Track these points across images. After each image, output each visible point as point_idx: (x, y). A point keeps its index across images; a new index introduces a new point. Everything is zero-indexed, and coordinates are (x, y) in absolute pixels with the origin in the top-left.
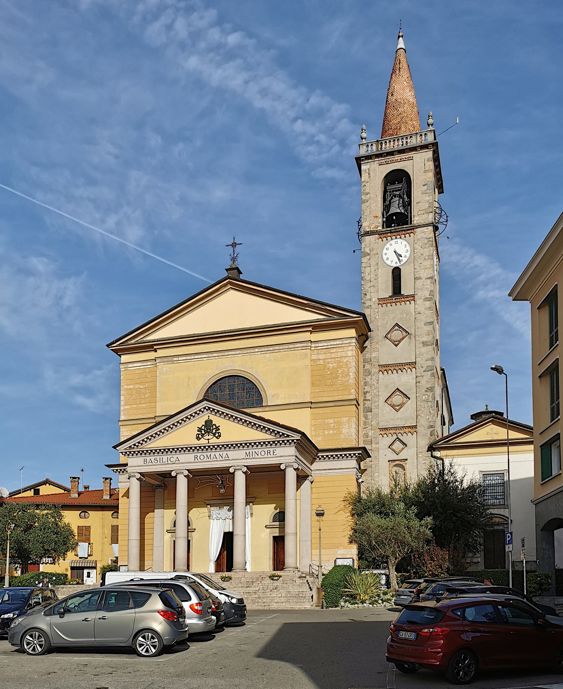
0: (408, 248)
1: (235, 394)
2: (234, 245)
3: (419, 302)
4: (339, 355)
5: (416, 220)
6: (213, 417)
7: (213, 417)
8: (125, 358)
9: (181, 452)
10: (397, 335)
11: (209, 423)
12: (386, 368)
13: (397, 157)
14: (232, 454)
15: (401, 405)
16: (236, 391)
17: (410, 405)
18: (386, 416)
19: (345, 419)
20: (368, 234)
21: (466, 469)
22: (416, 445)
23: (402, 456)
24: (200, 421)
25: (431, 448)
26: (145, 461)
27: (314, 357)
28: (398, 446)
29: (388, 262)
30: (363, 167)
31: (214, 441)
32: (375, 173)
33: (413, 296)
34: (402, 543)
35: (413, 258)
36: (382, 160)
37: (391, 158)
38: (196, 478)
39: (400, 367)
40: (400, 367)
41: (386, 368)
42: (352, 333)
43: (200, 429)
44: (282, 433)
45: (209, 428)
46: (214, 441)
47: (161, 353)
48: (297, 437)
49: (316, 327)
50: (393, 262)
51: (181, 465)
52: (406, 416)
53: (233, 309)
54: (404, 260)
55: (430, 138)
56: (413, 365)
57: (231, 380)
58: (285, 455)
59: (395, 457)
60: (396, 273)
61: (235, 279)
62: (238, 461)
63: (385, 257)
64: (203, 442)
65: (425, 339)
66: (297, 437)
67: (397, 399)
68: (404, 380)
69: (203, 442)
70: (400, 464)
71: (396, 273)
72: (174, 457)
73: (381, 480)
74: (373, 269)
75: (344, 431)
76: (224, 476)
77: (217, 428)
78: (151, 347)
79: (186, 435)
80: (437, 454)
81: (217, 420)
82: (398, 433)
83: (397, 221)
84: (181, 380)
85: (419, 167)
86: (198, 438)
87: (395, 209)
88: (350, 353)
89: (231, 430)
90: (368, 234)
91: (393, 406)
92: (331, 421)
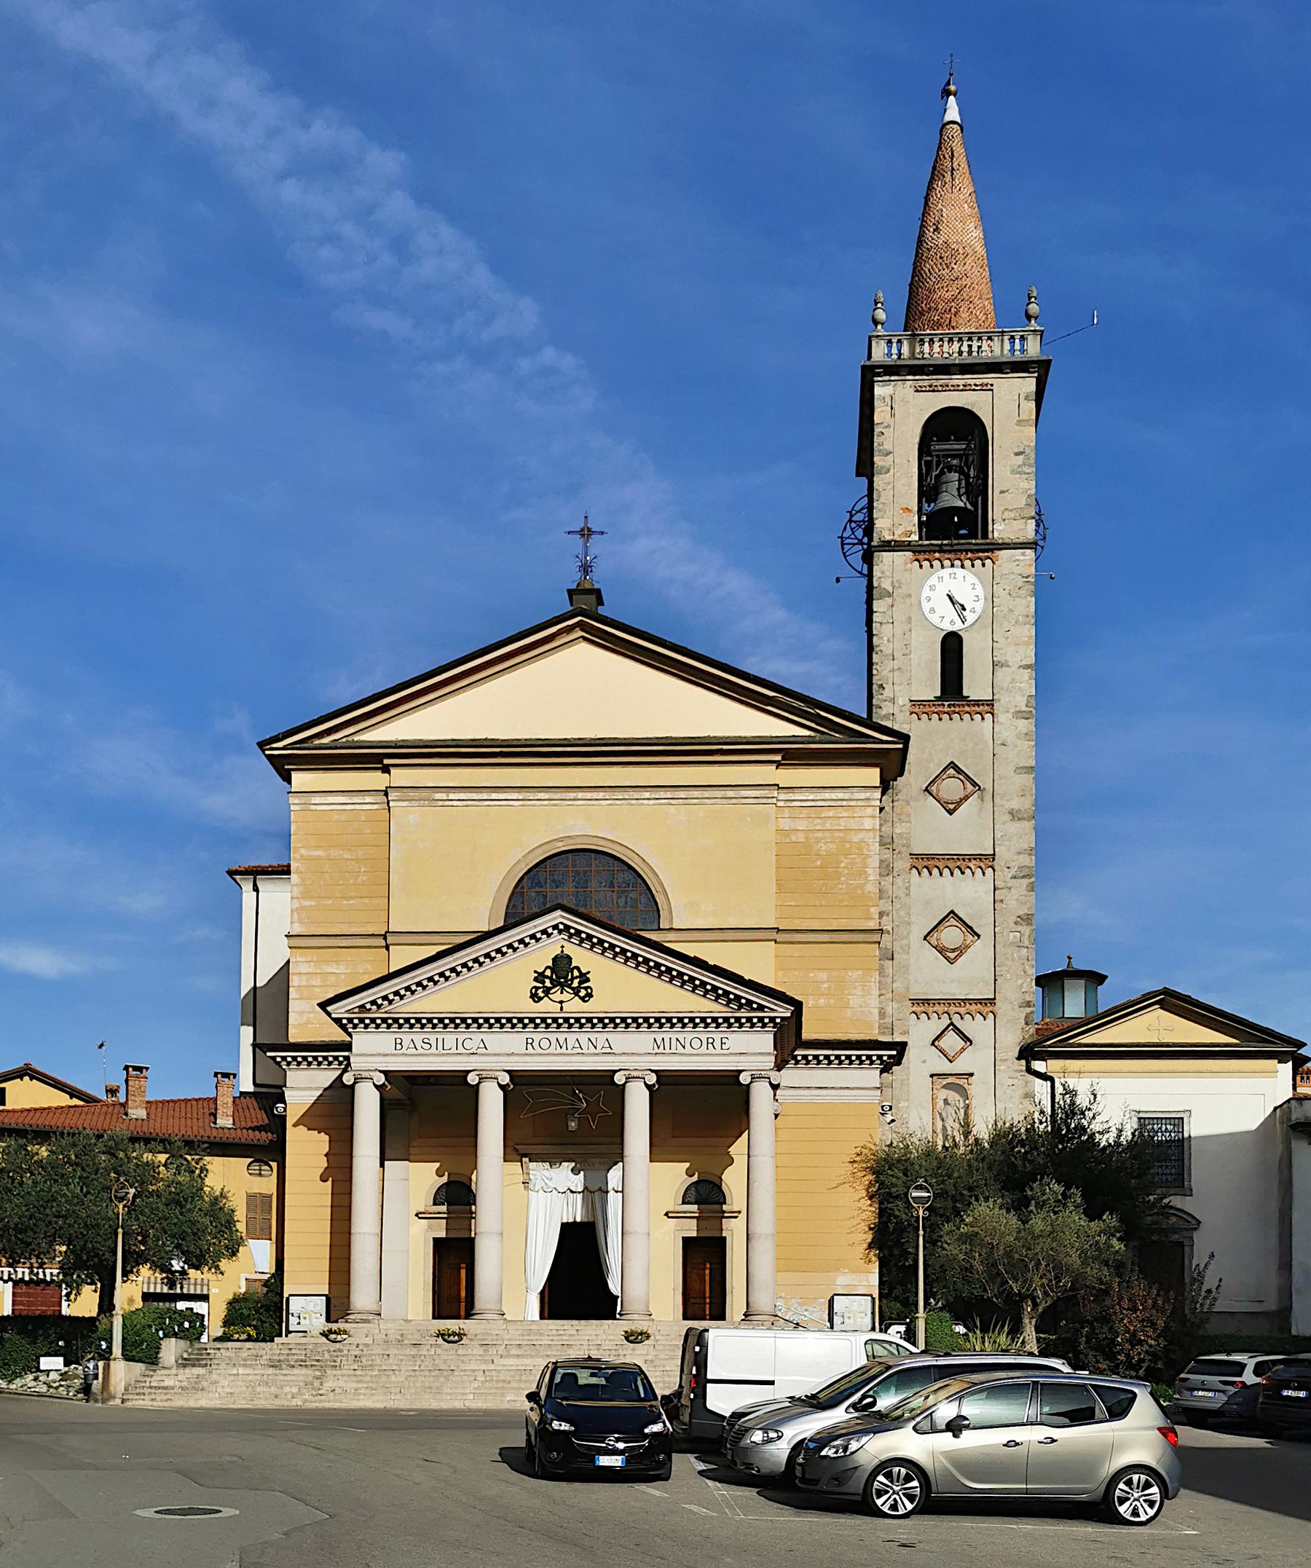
0: (980, 591)
1: (588, 893)
2: (586, 533)
3: (1002, 717)
4: (843, 824)
5: (999, 531)
8: (301, 779)
9: (492, 1029)
10: (951, 788)
11: (561, 966)
12: (927, 862)
13: (958, 380)
15: (960, 951)
16: (593, 885)
17: (980, 953)
18: (928, 973)
19: (854, 974)
20: (889, 546)
21: (1116, 1101)
22: (992, 1046)
23: (960, 1066)
24: (542, 956)
25: (1028, 1053)
26: (398, 1044)
27: (785, 824)
28: (951, 1041)
29: (934, 619)
30: (879, 390)
31: (574, 1006)
32: (904, 411)
33: (990, 703)
34: (1059, 1269)
35: (992, 617)
36: (924, 380)
37: (942, 379)
38: (525, 1090)
39: (958, 862)
40: (958, 862)
41: (927, 862)
42: (872, 775)
43: (540, 977)
44: (740, 999)
45: (561, 974)
46: (574, 1006)
47: (400, 776)
48: (783, 1011)
49: (792, 755)
50: (948, 621)
51: (492, 1058)
52: (969, 976)
53: (580, 688)
54: (971, 617)
55: (1033, 349)
56: (986, 860)
57: (580, 859)
58: (748, 1050)
59: (945, 1067)
60: (952, 646)
61: (588, 614)
62: (635, 1058)
63: (926, 607)
64: (547, 1007)
65: (1015, 804)
66: (783, 1011)
67: (952, 936)
68: (969, 893)
69: (547, 1007)
70: (958, 1083)
71: (952, 646)
72: (474, 1038)
73: (919, 1118)
74: (899, 630)
75: (854, 1001)
76: (602, 1091)
77: (584, 978)
78: (375, 759)
79: (506, 983)
80: (1039, 1066)
81: (582, 958)
82: (954, 1011)
83: (955, 528)
84: (456, 855)
85: (1005, 407)
86: (535, 997)
87: (952, 498)
88: (868, 824)
89: (617, 984)
90: (889, 546)
91: (942, 950)
92: (824, 976)
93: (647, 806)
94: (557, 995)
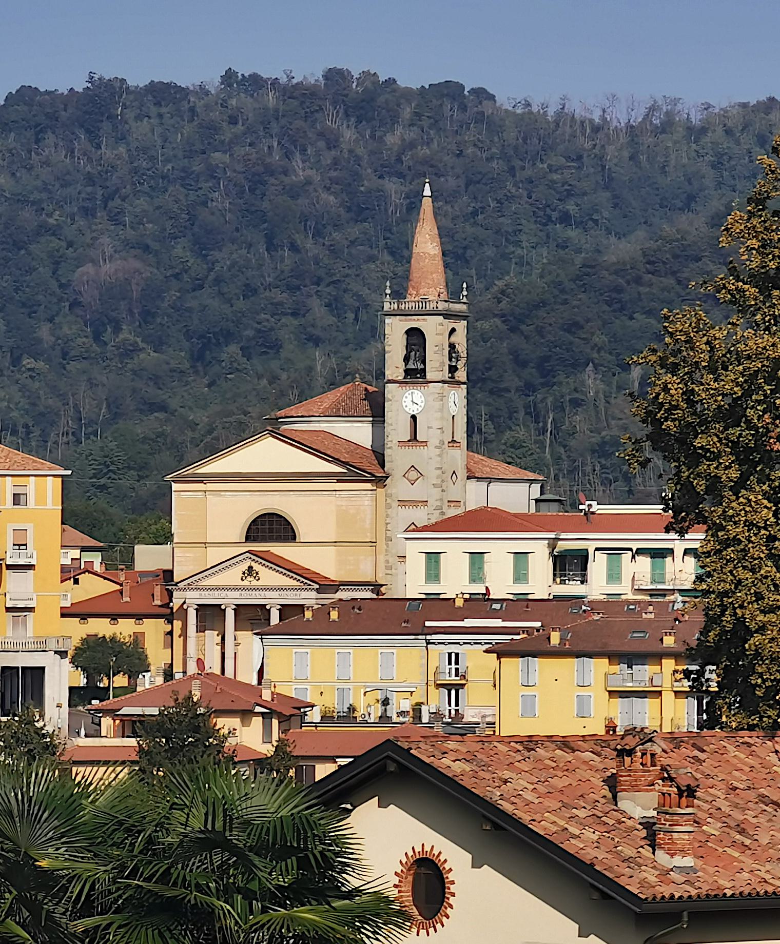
4: (358, 503)
6: (253, 564)
7: (253, 564)
10: (413, 475)
11: (250, 568)
12: (403, 503)
14: (269, 594)
19: (362, 557)
24: (244, 566)
26: (201, 595)
27: (339, 503)
29: (407, 409)
31: (255, 583)
39: (414, 503)
40: (414, 503)
41: (403, 503)
43: (244, 573)
46: (255, 583)
47: (210, 486)
49: (339, 478)
62: (274, 601)
63: (404, 405)
64: (246, 583)
69: (246, 583)
72: (224, 594)
79: (233, 577)
81: (256, 567)
86: (242, 579)
88: (366, 503)
90: (390, 381)
92: (351, 558)
93: (292, 497)
94: (249, 578)
